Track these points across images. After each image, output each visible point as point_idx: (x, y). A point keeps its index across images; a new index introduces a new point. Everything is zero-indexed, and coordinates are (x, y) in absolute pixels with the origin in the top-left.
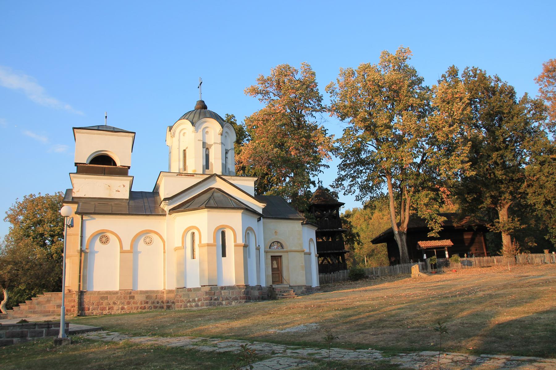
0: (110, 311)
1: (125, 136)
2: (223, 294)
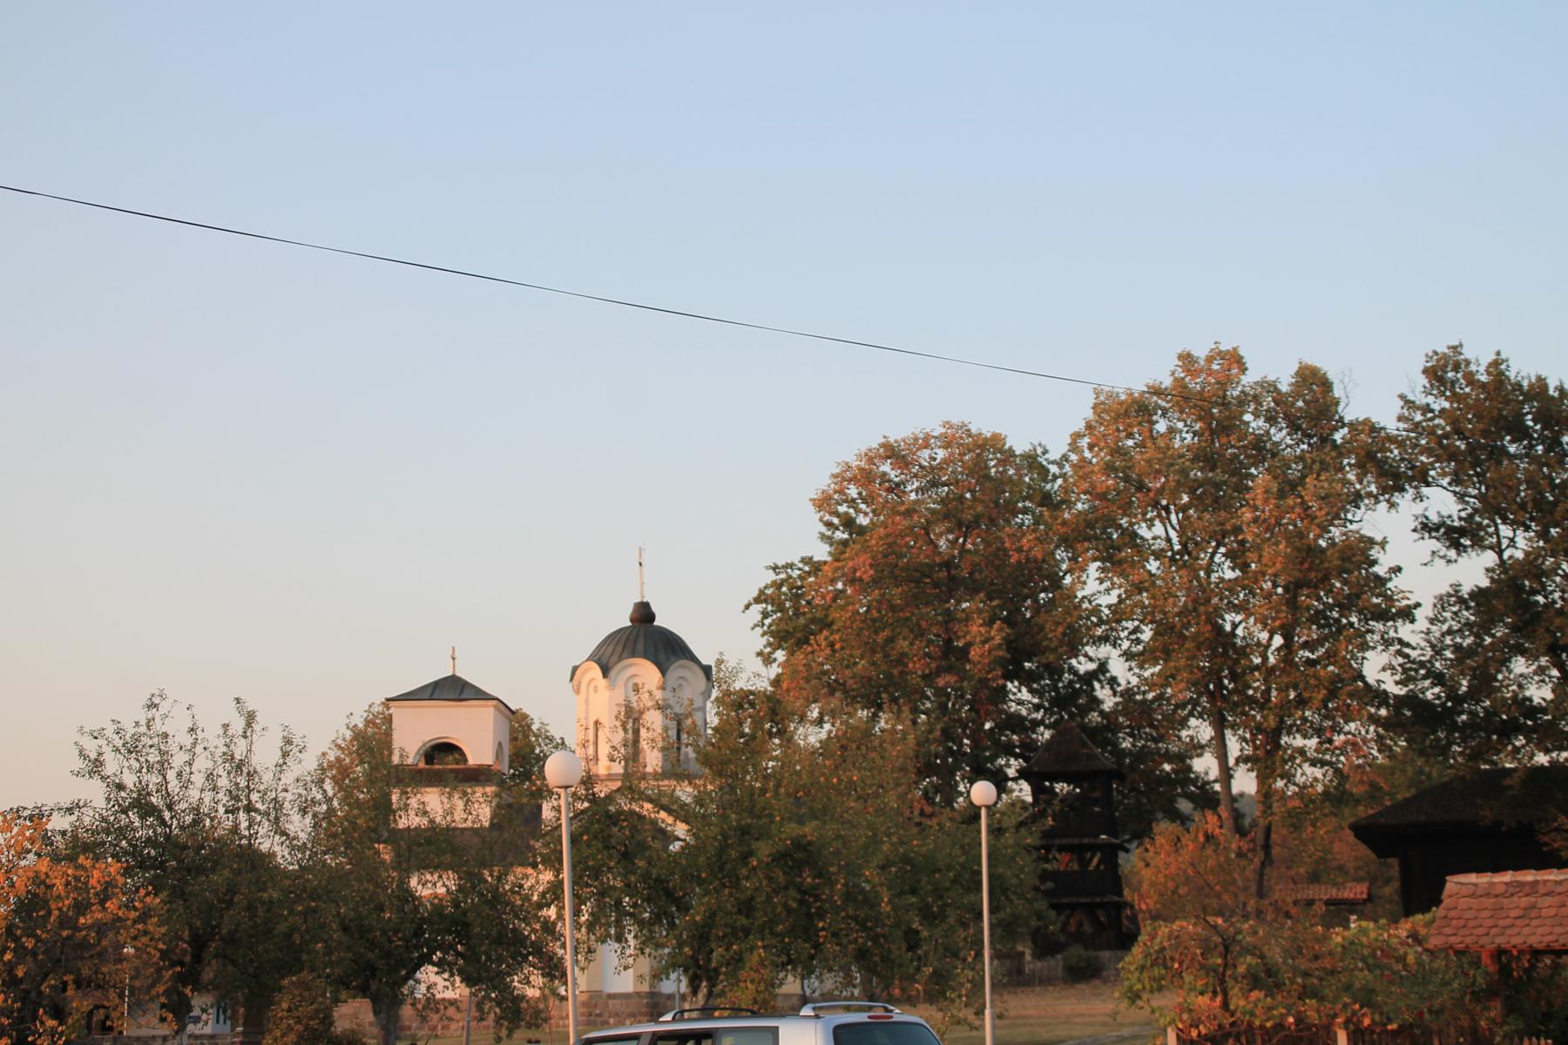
0: (444, 1031)
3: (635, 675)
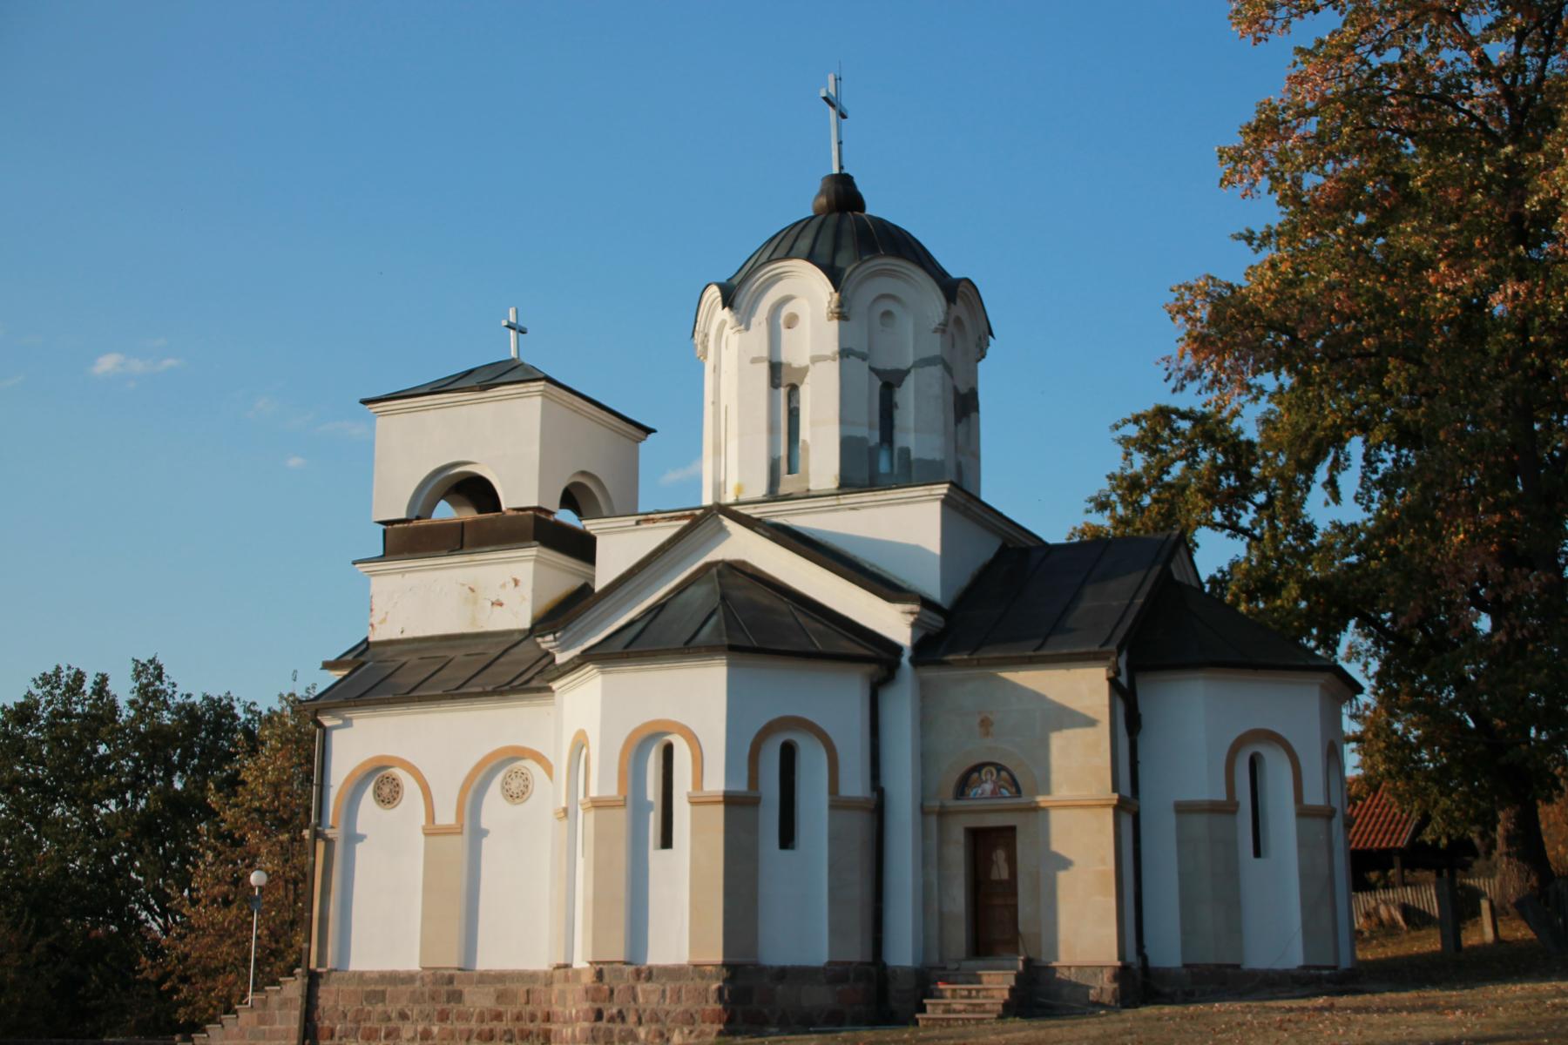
1: (520, 396)
2: (641, 1000)
3: (786, 300)
